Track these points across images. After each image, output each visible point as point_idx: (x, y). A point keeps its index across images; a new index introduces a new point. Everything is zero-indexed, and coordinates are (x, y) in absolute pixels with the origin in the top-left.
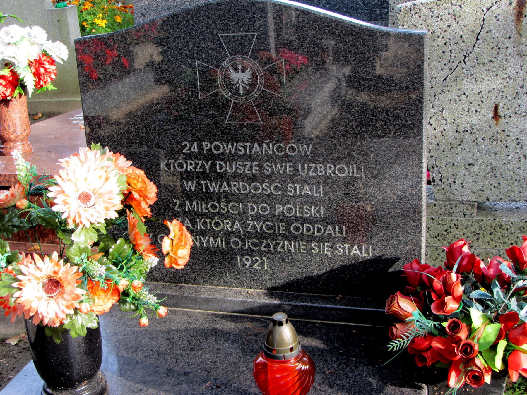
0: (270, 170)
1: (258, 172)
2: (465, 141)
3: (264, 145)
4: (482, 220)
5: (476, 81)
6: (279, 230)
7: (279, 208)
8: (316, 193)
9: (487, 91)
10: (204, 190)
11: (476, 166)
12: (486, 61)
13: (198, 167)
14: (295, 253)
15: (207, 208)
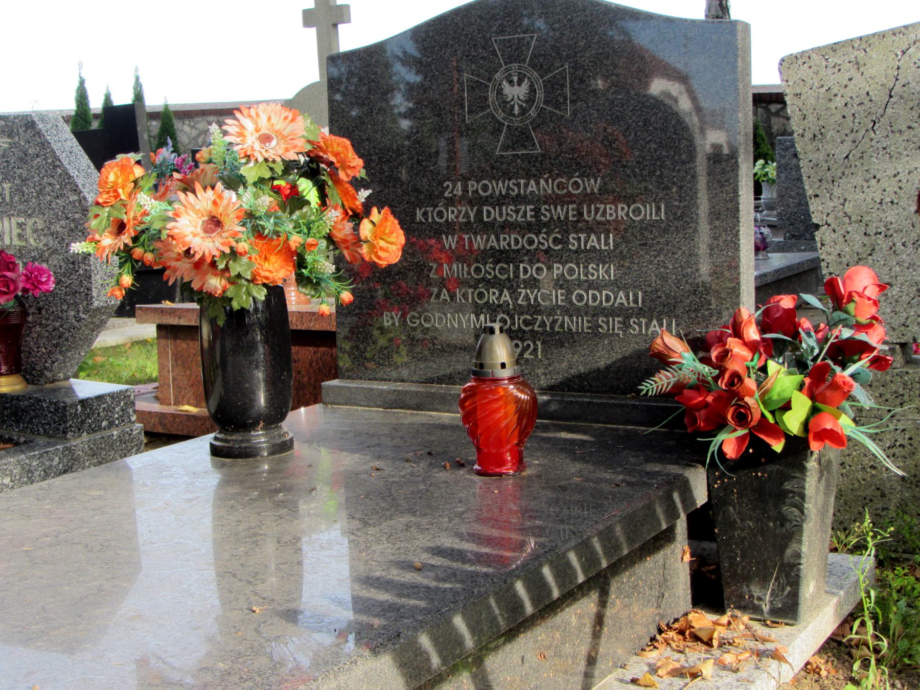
0: (548, 215)
1: (533, 219)
2: (877, 248)
3: (542, 182)
4: (907, 373)
5: (891, 157)
6: (557, 301)
7: (558, 268)
8: (605, 245)
9: (907, 171)
10: (467, 247)
11: (895, 287)
12: (904, 128)
13: (461, 216)
14: (577, 333)
15: (469, 273)
